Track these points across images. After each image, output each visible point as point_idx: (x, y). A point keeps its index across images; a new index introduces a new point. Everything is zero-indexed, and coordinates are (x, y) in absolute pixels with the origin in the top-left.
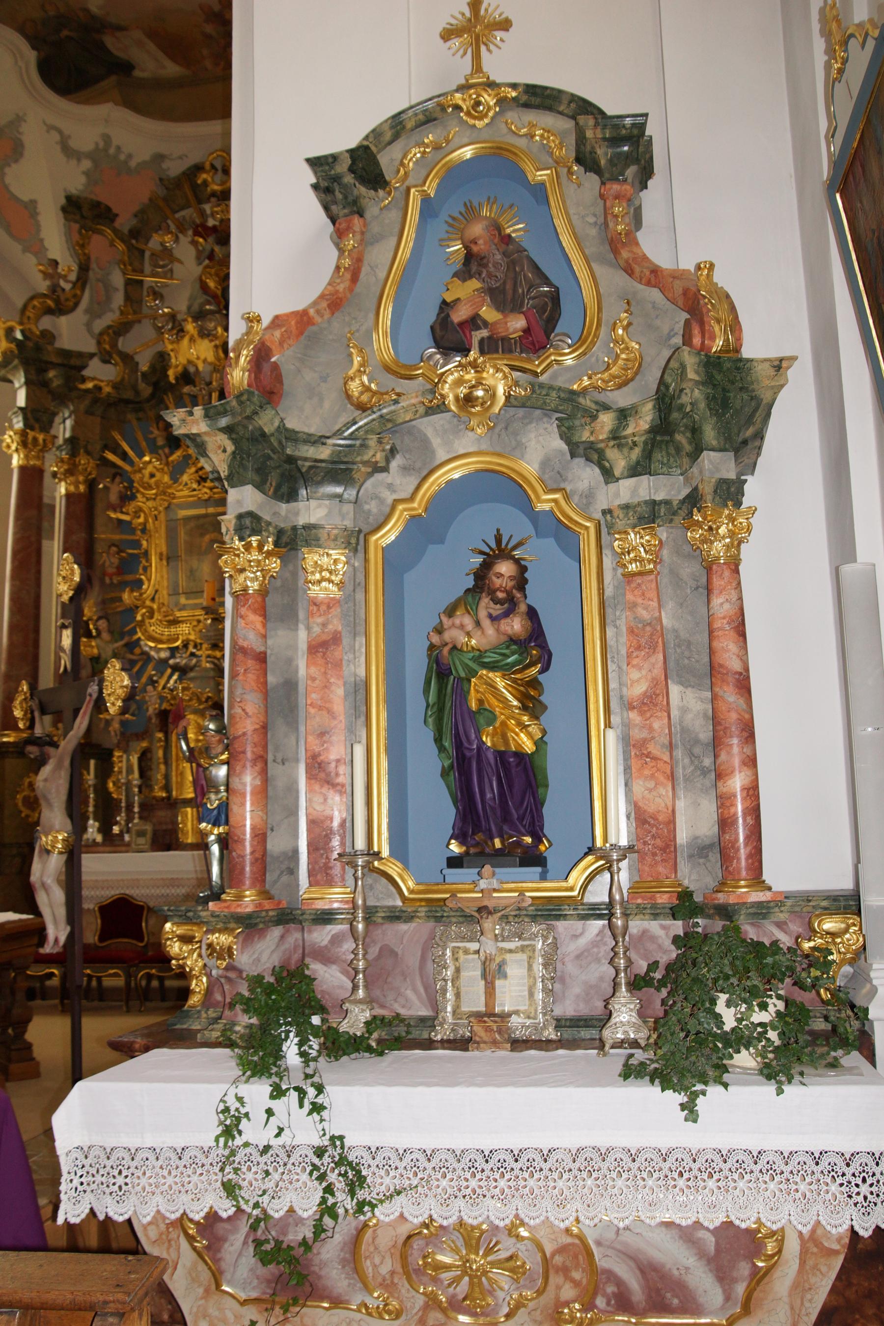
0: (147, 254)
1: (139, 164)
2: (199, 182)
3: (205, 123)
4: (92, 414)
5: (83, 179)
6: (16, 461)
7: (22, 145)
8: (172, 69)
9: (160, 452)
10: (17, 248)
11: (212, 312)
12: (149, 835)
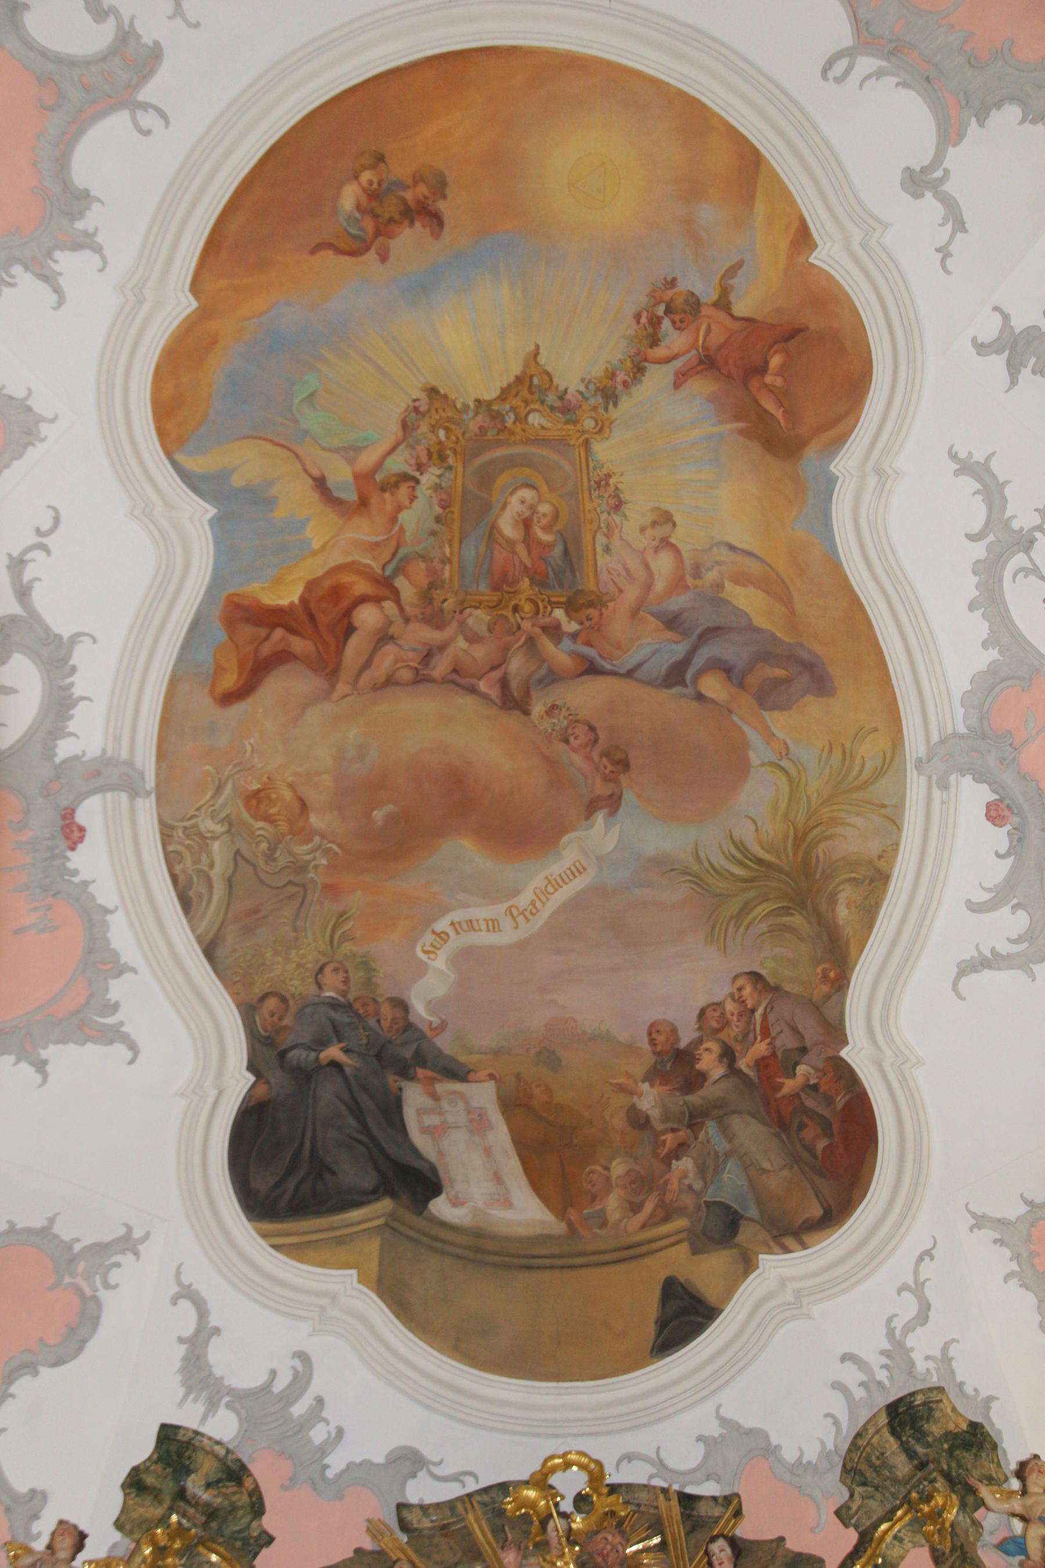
1: (351, 1466)
7: (95, 1321)
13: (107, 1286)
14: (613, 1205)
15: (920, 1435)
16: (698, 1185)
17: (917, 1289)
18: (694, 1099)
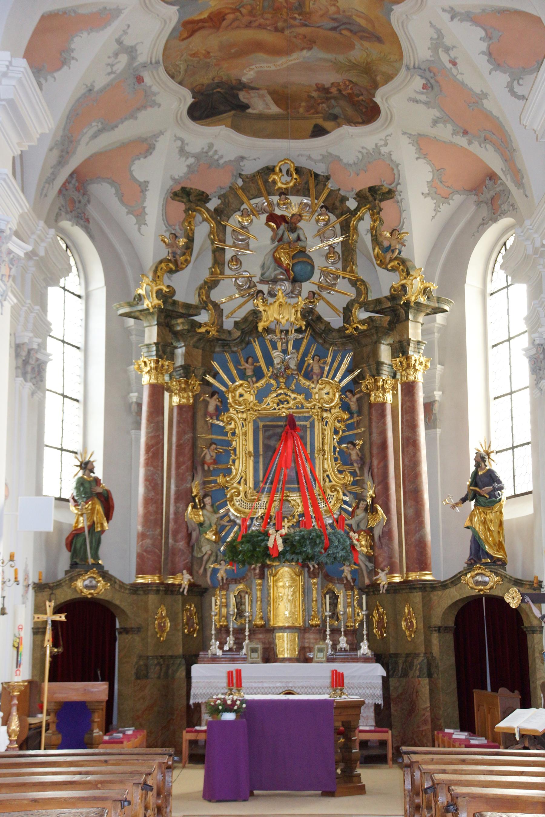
0: (229, 230)
1: (225, 162)
2: (270, 180)
3: (281, 140)
4: (197, 348)
5: (185, 170)
6: (146, 379)
8: (274, 109)
9: (249, 380)
10: (124, 210)
11: (282, 280)
12: (260, 651)
13: (156, 141)
14: (301, 110)
15: (376, 193)
16: (327, 109)
17: (386, 140)
18: (329, 96)
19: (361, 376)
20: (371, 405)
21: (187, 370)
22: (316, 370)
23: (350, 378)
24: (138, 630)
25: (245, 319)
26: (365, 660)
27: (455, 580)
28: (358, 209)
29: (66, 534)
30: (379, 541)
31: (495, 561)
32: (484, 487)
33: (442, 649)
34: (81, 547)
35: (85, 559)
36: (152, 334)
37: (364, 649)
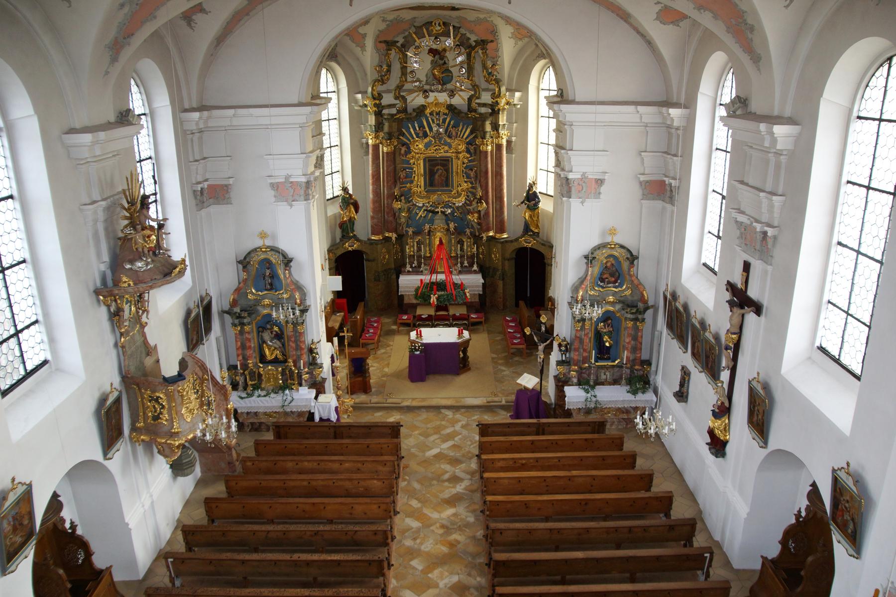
10: (354, 45)
19: (476, 137)
20: (480, 152)
21: (390, 136)
22: (454, 134)
23: (472, 137)
24: (374, 260)
25: (418, 108)
26: (475, 272)
27: (517, 240)
28: (475, 46)
29: (338, 222)
30: (483, 217)
31: (534, 233)
32: (532, 198)
33: (510, 269)
34: (346, 228)
35: (348, 233)
36: (372, 120)
37: (475, 268)
